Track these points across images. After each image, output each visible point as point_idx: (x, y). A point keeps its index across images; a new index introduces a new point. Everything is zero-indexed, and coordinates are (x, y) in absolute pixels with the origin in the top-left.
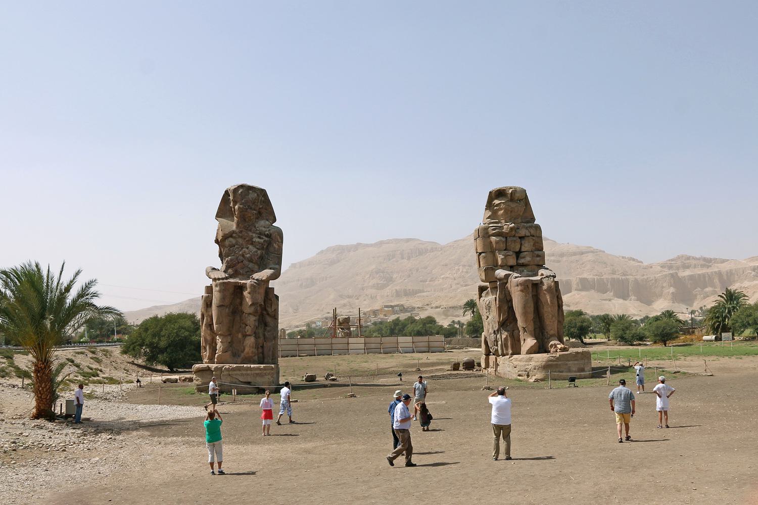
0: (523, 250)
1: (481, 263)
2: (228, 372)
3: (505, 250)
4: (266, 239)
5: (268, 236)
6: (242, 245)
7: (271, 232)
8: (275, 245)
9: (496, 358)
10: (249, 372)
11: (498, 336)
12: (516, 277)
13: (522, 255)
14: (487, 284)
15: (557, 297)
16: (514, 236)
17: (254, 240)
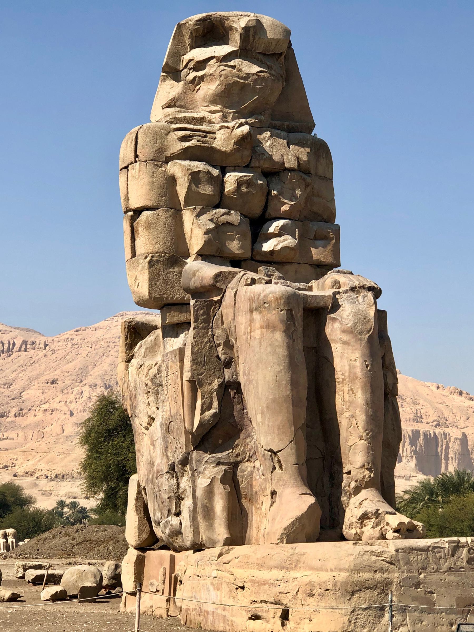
0: (271, 212)
1: (138, 243)
3: (217, 207)
9: (172, 559)
11: (185, 483)
12: (253, 282)
14: (154, 317)
15: (383, 358)
16: (247, 166)
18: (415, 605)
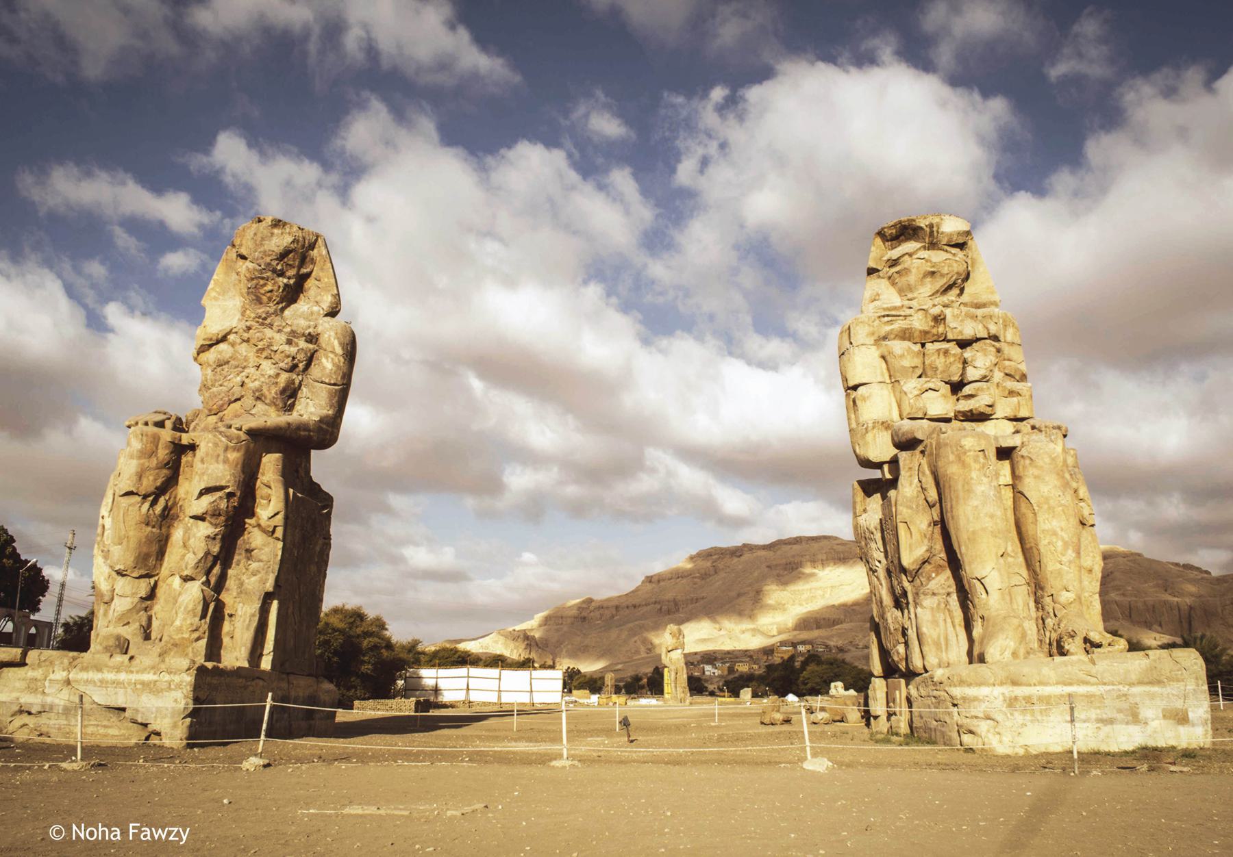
2: (65, 674)
4: (302, 344)
5: (312, 338)
6: (246, 359)
7: (320, 329)
8: (324, 360)
10: (123, 676)
13: (967, 390)
17: (275, 348)
18: (1120, 716)
